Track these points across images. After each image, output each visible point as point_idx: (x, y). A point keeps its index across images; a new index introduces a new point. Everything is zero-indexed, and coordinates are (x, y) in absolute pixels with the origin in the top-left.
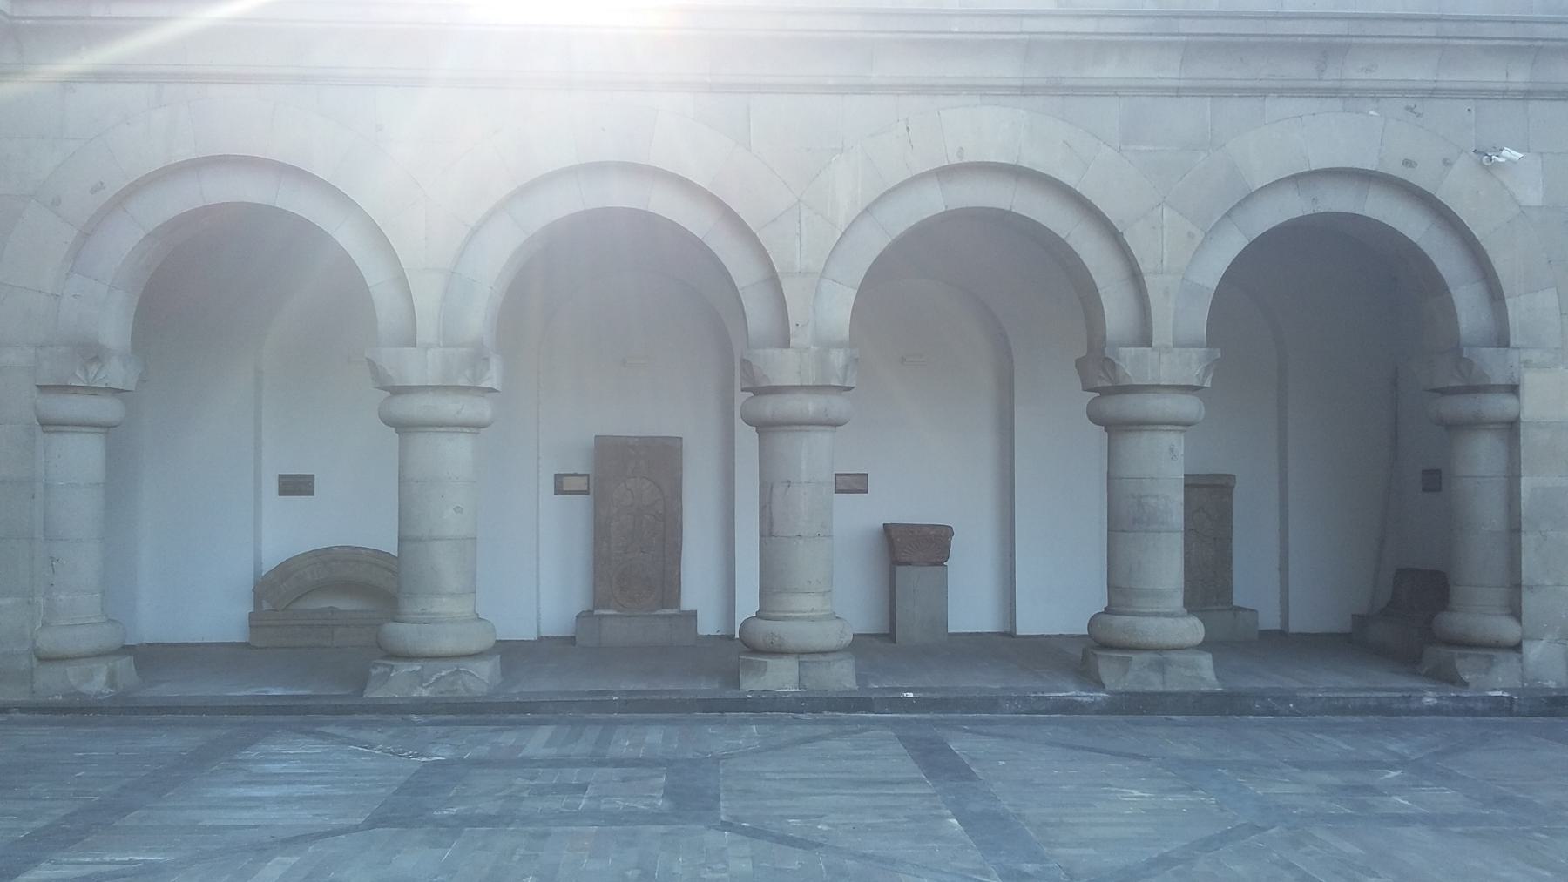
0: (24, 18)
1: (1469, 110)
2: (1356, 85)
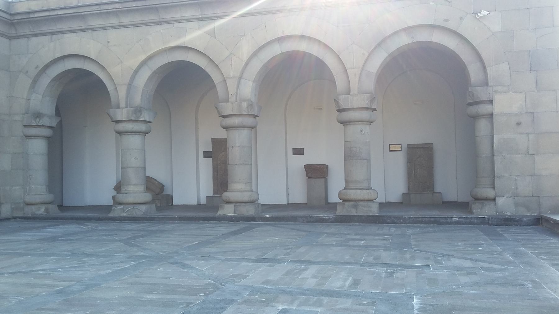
0: (14, 20)
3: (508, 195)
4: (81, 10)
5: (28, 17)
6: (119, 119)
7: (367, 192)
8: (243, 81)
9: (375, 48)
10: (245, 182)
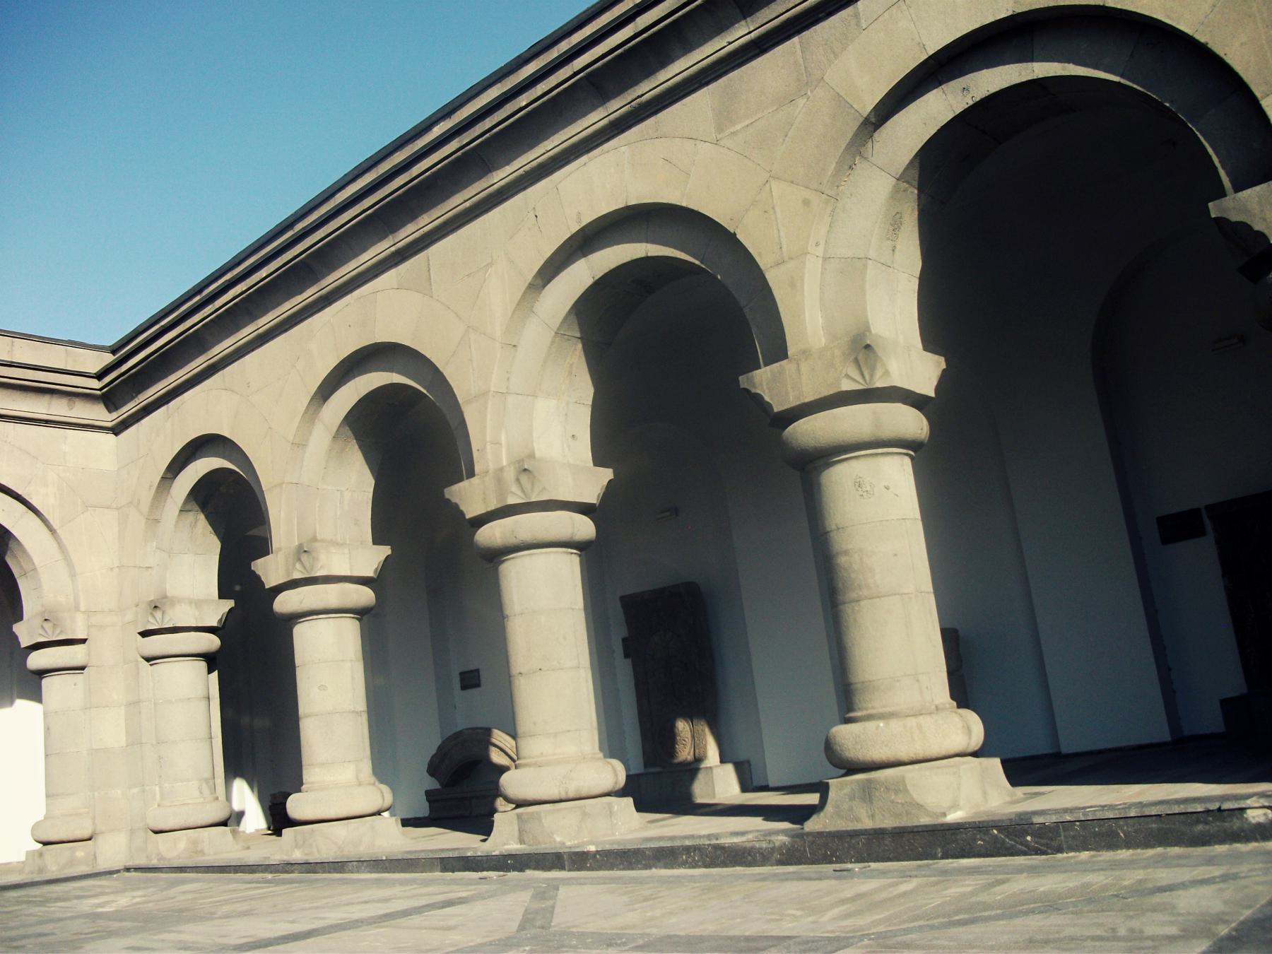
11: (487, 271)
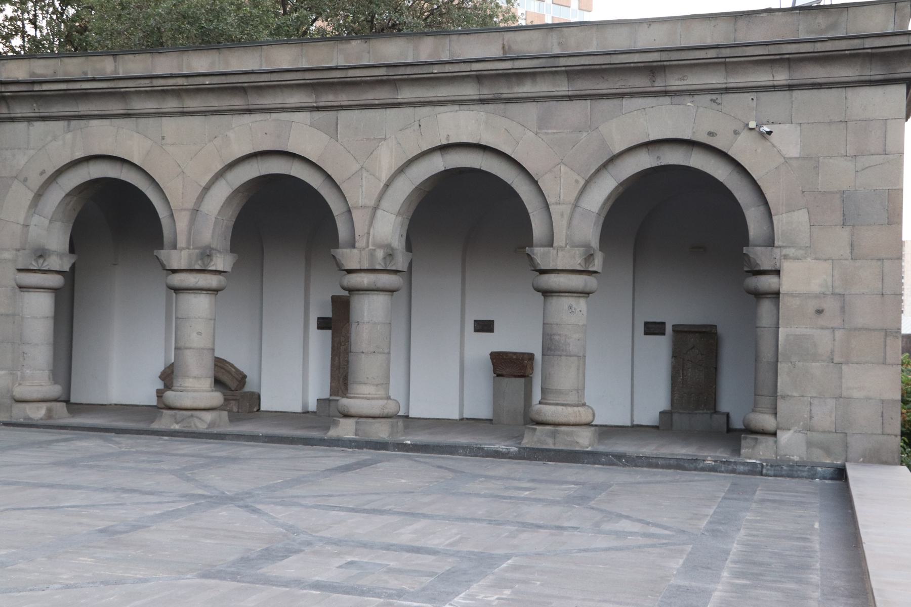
1: (752, 99)
2: (675, 88)
3: (796, 428)
4: (121, 84)
5: (31, 89)
6: (175, 266)
7: (574, 411)
8: (379, 213)
9: (598, 171)
10: (375, 383)
11: (380, 142)
